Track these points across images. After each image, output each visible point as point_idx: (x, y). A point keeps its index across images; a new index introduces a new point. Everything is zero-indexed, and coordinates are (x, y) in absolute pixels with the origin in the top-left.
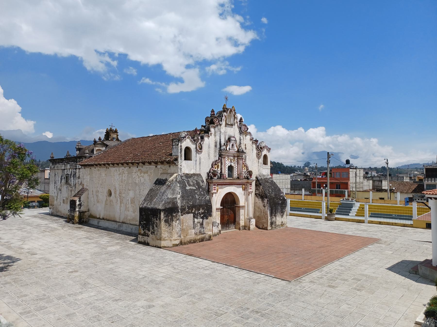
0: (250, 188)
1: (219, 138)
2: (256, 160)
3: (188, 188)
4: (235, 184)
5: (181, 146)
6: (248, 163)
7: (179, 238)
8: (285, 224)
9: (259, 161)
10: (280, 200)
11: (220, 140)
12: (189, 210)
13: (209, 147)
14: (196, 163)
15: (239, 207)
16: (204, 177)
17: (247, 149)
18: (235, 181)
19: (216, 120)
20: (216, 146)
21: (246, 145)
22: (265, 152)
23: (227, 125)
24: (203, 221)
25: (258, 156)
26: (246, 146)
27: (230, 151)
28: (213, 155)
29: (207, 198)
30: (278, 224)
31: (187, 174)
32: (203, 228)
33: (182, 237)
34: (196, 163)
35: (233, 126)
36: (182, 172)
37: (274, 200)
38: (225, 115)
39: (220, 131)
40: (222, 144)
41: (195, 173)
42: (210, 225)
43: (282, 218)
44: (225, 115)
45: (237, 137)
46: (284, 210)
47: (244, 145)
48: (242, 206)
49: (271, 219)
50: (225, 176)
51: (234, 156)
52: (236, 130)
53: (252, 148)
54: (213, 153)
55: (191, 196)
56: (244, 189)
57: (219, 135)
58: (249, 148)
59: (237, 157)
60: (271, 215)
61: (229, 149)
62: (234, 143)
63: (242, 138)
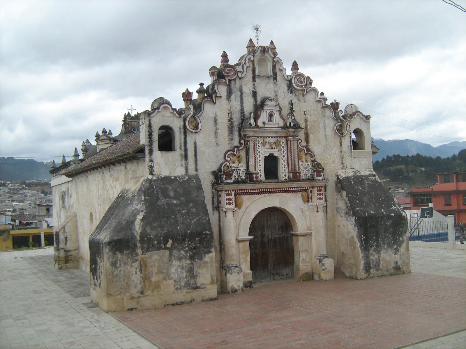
3: (162, 202)
6: (316, 148)
11: (242, 107)
15: (297, 235)
16: (206, 181)
19: (228, 70)
22: (355, 124)
27: (266, 126)
38: (249, 59)
40: (247, 113)
44: (249, 59)
45: (284, 99)
48: (300, 234)
50: (254, 176)
52: (279, 86)
56: (307, 200)
58: (315, 119)
59: (285, 137)
61: (264, 123)
62: (275, 112)
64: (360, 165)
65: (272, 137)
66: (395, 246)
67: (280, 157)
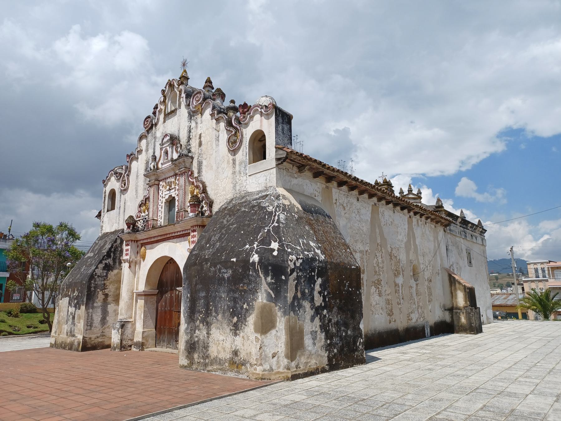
1: (152, 150)
2: (226, 161)
8: (248, 365)
9: (234, 161)
10: (227, 264)
11: (154, 153)
13: (137, 176)
14: (119, 212)
21: (202, 135)
26: (202, 139)
27: (163, 166)
28: (142, 186)
30: (215, 354)
31: (108, 233)
32: (74, 326)
33: (57, 335)
34: (119, 212)
36: (103, 232)
39: (155, 138)
41: (117, 229)
43: (236, 335)
46: (245, 306)
47: (198, 137)
49: (191, 331)
53: (217, 133)
57: (153, 146)
60: (191, 318)
62: (168, 148)
63: (193, 124)
64: (256, 185)
65: (171, 177)
66: (235, 319)
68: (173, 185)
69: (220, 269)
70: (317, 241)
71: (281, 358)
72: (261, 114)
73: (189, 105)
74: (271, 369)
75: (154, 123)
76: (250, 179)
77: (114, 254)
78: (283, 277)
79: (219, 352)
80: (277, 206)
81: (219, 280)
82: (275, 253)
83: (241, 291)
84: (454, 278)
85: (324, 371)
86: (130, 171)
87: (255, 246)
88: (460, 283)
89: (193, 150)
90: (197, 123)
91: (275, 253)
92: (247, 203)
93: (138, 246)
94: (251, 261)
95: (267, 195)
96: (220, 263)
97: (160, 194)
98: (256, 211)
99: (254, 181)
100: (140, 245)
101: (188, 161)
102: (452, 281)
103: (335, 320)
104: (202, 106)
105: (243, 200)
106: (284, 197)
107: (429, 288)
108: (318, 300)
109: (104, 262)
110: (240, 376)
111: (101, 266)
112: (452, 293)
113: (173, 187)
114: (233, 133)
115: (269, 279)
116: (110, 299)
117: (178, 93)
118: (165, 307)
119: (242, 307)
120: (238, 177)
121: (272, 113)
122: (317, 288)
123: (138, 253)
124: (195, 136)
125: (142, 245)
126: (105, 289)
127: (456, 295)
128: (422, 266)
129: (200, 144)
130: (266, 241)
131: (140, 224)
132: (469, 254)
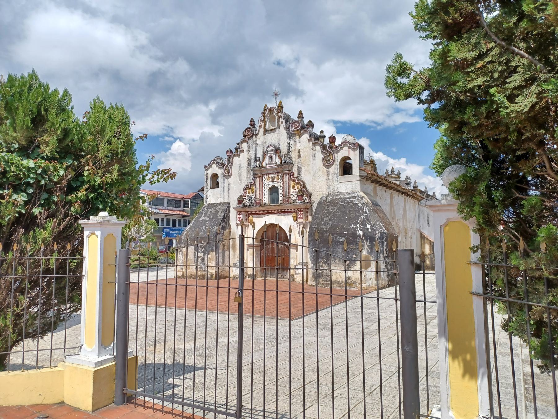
0: (300, 216)
1: (254, 152)
2: (321, 170)
4: (279, 213)
5: (207, 174)
7: (181, 270)
9: (328, 172)
10: (341, 235)
11: (256, 155)
12: (191, 242)
13: (240, 168)
14: (224, 190)
17: (302, 156)
18: (280, 208)
20: (249, 165)
23: (266, 131)
24: (204, 255)
25: (328, 163)
26: (301, 153)
27: (267, 166)
28: (246, 176)
29: (212, 231)
31: (213, 204)
34: (224, 190)
35: (277, 130)
36: (208, 202)
37: (323, 235)
39: (256, 144)
41: (222, 202)
42: (212, 261)
47: (297, 151)
51: (278, 173)
53: (314, 153)
54: (246, 174)
55: (199, 227)
57: (254, 149)
58: (306, 154)
62: (273, 155)
63: (292, 142)
67: (279, 187)
68: (275, 179)
69: (336, 237)
70: (383, 222)
71: (373, 281)
72: (349, 147)
73: (289, 128)
74: (370, 286)
75: (255, 134)
76: (340, 185)
77: (226, 219)
78: (374, 243)
79: (337, 278)
80: (363, 204)
81: (335, 243)
82: (370, 230)
83: (351, 249)
84: (424, 236)
85: (387, 287)
86: (232, 163)
87: (358, 226)
88: (427, 239)
89: (293, 159)
90: (295, 142)
91: (370, 230)
92: (344, 200)
93: (246, 215)
94: (358, 234)
95: (356, 197)
96: (337, 234)
97: (264, 183)
98: (352, 206)
99: (343, 186)
100: (247, 215)
101: (291, 166)
102: (422, 237)
103: (390, 263)
104: (300, 132)
105: (338, 197)
106: (365, 199)
107: (411, 242)
108: (385, 253)
109: (222, 224)
110: (352, 289)
111: (221, 227)
112: (422, 245)
113: (275, 180)
114: (328, 155)
115: (368, 243)
116: (226, 248)
117: (277, 117)
118: (268, 253)
119: (352, 257)
120: (331, 182)
121: (357, 148)
122: (385, 247)
123: (246, 220)
124: (295, 150)
125: (249, 215)
126: (223, 241)
127: (424, 247)
128: (408, 229)
129: (299, 156)
130: (363, 224)
131: (246, 202)
132: (428, 217)
